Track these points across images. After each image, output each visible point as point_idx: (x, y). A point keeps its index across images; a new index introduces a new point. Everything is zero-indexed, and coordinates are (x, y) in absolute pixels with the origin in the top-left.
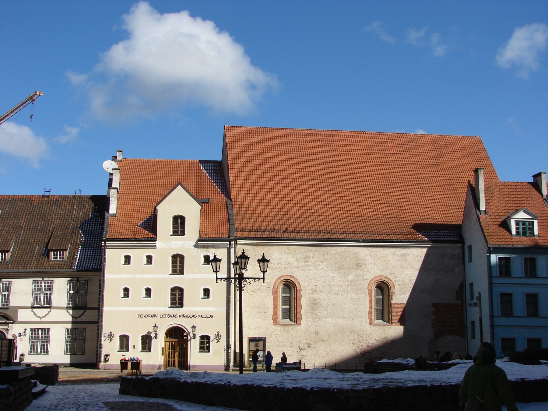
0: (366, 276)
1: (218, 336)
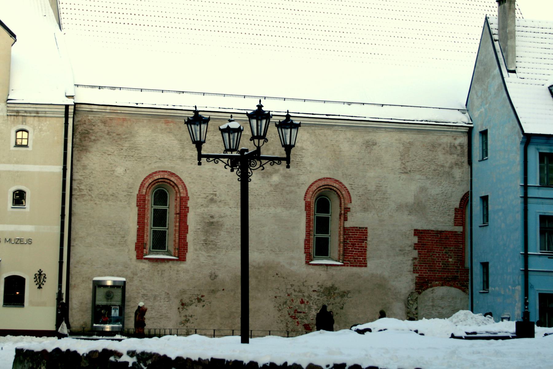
0: (303, 178)
1: (40, 278)
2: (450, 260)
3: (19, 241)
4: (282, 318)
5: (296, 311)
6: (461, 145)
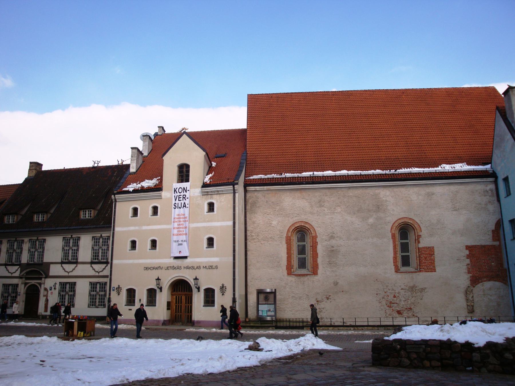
0: (388, 219)
1: (223, 288)
2: (493, 264)
3: (211, 267)
4: (382, 308)
5: (391, 303)
6: (491, 190)
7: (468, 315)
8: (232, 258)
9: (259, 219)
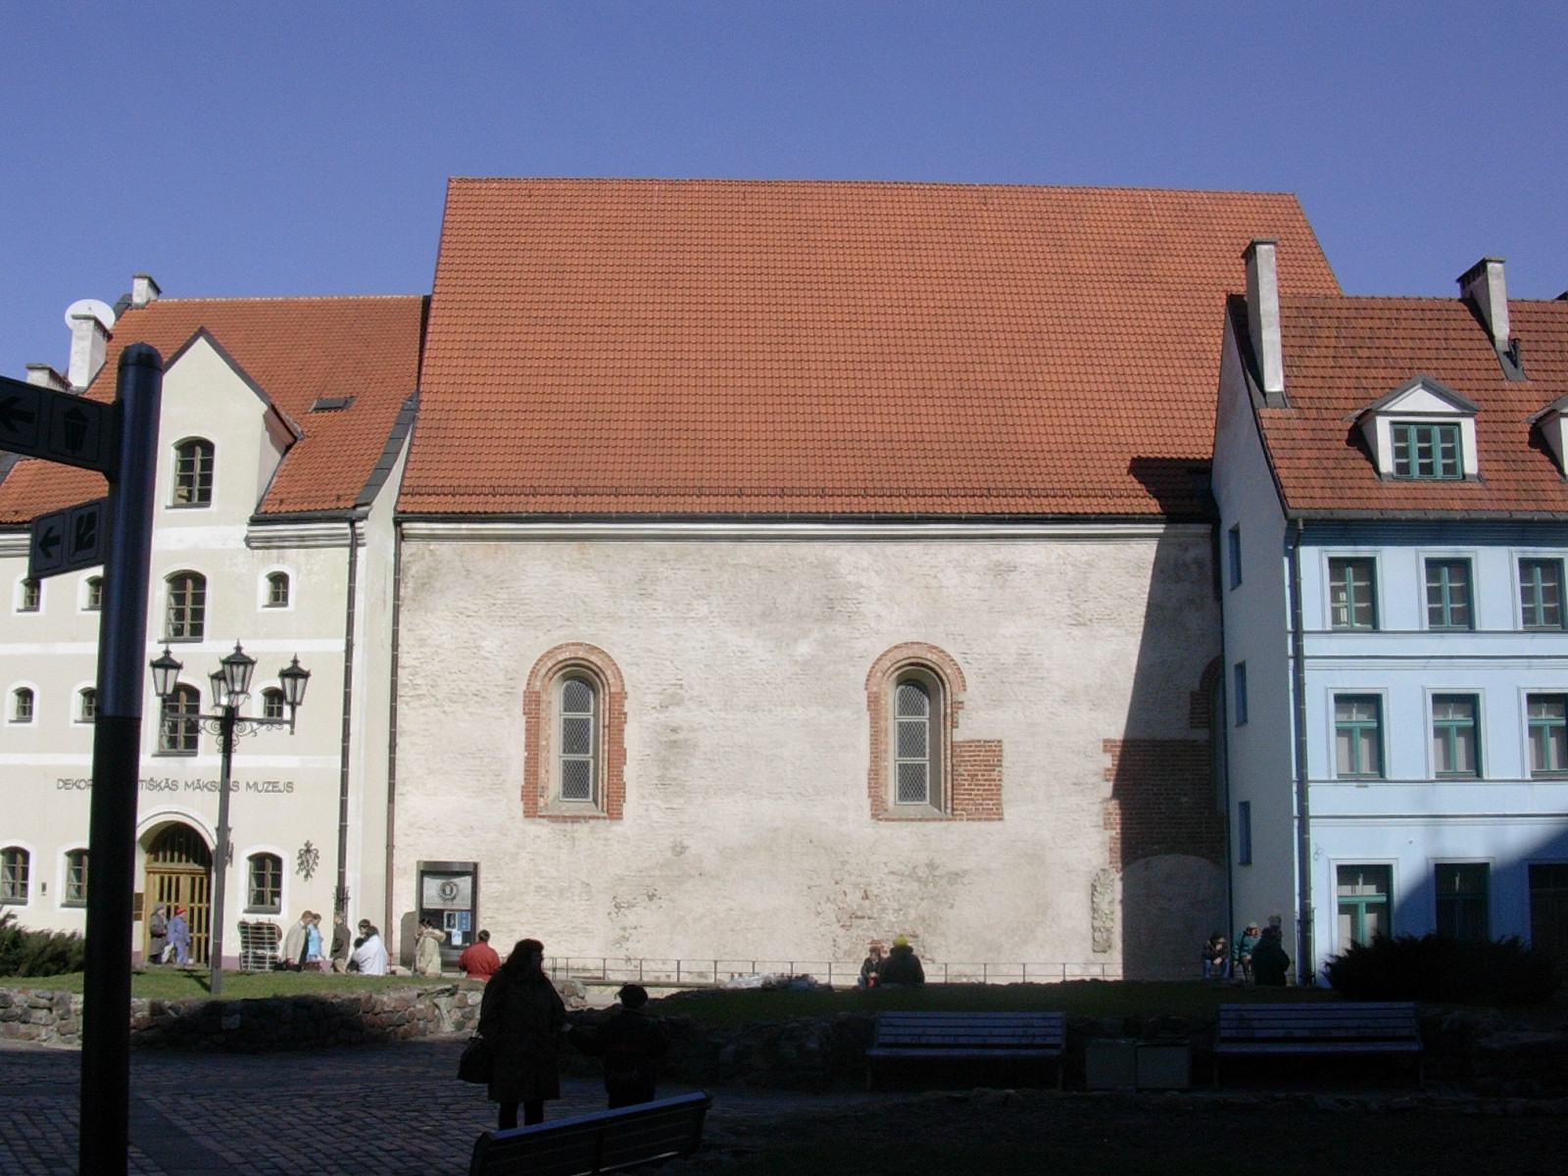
2: (1184, 799)
3: (273, 786)
4: (822, 929)
5: (853, 916)
6: (1199, 563)
7: (1092, 957)
8: (339, 758)
9: (434, 631)
